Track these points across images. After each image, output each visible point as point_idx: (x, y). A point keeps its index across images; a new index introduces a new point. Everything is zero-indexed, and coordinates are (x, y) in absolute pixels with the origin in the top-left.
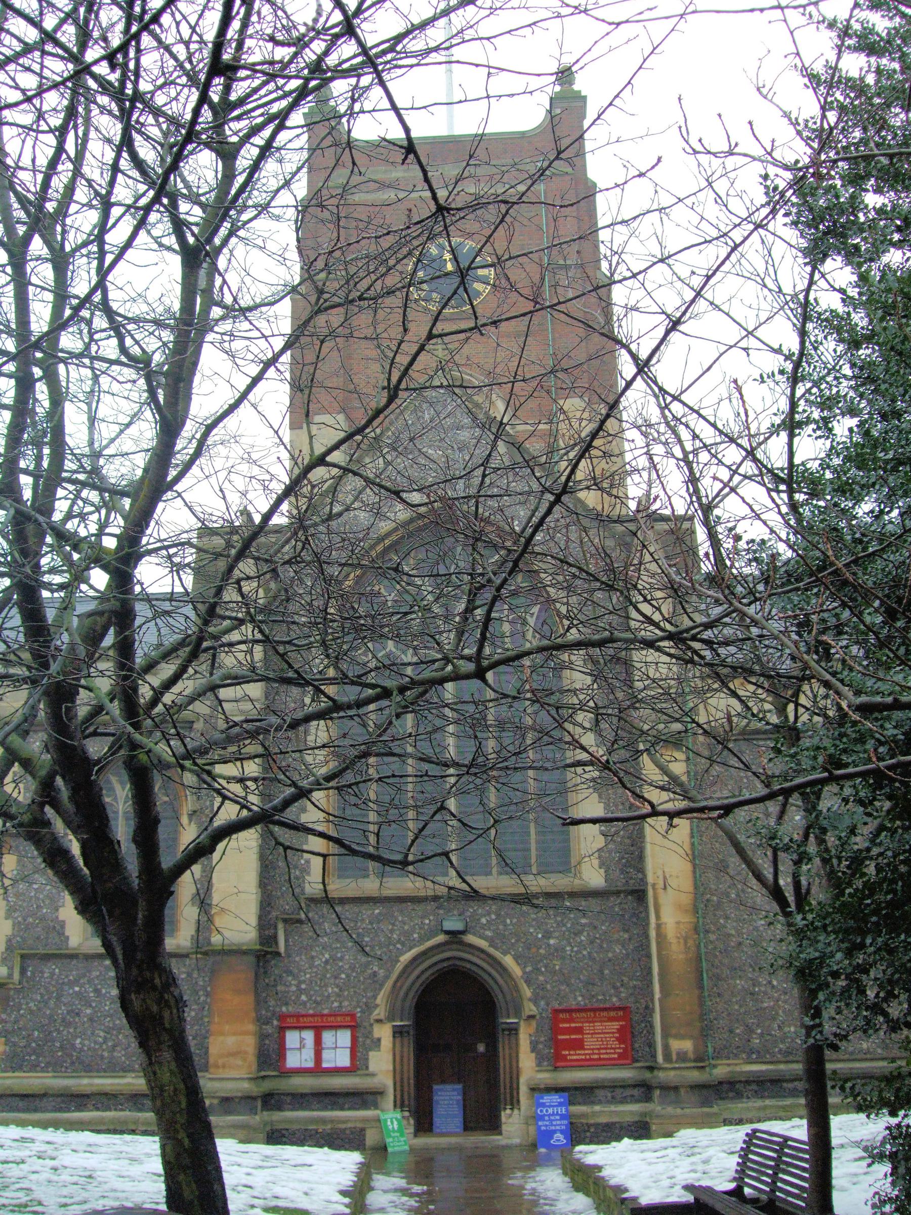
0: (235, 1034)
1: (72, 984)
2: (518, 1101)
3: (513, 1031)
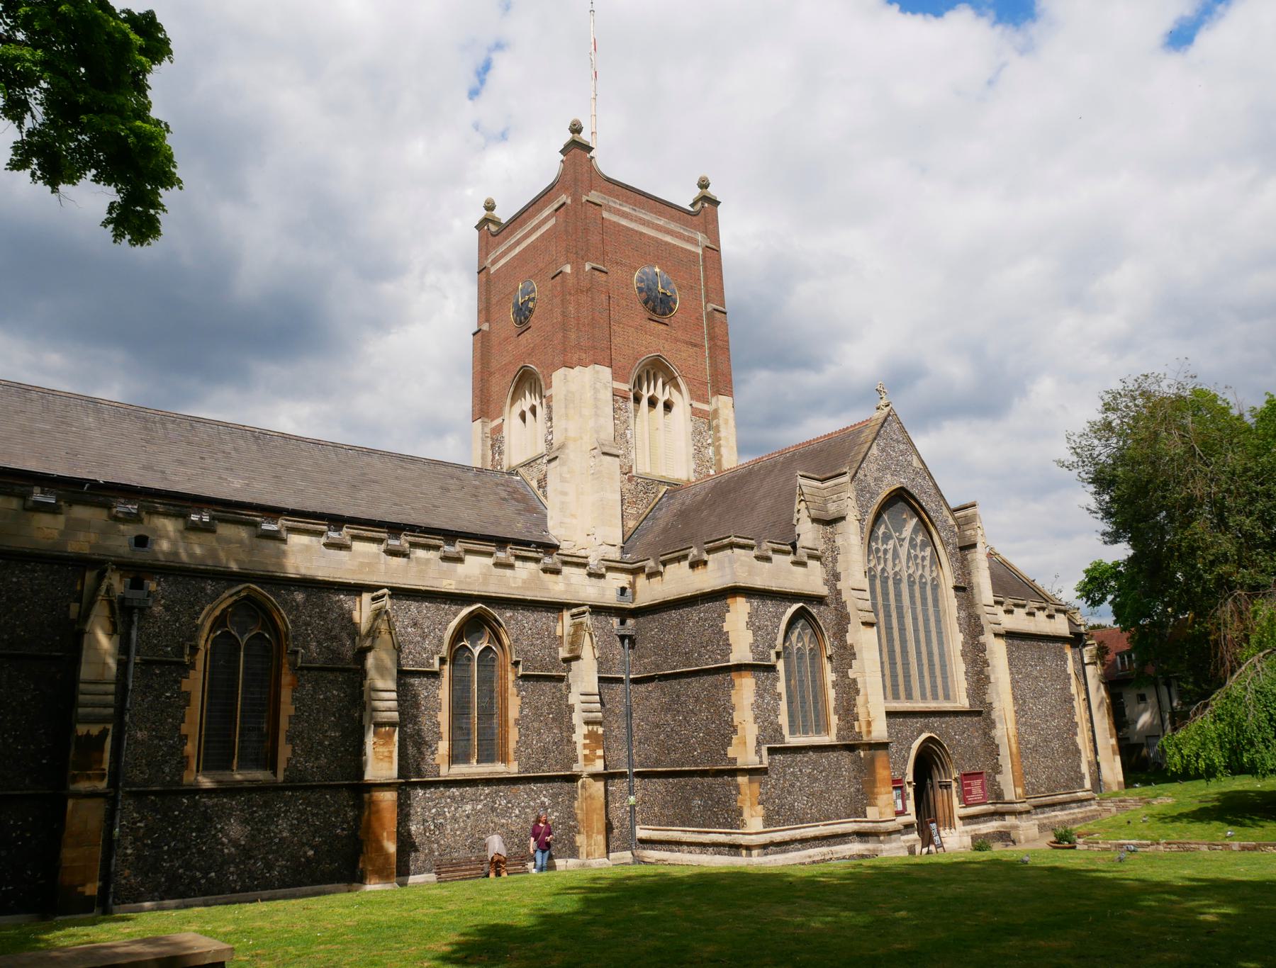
0: (886, 793)
1: (789, 766)
2: (954, 824)
3: (948, 786)
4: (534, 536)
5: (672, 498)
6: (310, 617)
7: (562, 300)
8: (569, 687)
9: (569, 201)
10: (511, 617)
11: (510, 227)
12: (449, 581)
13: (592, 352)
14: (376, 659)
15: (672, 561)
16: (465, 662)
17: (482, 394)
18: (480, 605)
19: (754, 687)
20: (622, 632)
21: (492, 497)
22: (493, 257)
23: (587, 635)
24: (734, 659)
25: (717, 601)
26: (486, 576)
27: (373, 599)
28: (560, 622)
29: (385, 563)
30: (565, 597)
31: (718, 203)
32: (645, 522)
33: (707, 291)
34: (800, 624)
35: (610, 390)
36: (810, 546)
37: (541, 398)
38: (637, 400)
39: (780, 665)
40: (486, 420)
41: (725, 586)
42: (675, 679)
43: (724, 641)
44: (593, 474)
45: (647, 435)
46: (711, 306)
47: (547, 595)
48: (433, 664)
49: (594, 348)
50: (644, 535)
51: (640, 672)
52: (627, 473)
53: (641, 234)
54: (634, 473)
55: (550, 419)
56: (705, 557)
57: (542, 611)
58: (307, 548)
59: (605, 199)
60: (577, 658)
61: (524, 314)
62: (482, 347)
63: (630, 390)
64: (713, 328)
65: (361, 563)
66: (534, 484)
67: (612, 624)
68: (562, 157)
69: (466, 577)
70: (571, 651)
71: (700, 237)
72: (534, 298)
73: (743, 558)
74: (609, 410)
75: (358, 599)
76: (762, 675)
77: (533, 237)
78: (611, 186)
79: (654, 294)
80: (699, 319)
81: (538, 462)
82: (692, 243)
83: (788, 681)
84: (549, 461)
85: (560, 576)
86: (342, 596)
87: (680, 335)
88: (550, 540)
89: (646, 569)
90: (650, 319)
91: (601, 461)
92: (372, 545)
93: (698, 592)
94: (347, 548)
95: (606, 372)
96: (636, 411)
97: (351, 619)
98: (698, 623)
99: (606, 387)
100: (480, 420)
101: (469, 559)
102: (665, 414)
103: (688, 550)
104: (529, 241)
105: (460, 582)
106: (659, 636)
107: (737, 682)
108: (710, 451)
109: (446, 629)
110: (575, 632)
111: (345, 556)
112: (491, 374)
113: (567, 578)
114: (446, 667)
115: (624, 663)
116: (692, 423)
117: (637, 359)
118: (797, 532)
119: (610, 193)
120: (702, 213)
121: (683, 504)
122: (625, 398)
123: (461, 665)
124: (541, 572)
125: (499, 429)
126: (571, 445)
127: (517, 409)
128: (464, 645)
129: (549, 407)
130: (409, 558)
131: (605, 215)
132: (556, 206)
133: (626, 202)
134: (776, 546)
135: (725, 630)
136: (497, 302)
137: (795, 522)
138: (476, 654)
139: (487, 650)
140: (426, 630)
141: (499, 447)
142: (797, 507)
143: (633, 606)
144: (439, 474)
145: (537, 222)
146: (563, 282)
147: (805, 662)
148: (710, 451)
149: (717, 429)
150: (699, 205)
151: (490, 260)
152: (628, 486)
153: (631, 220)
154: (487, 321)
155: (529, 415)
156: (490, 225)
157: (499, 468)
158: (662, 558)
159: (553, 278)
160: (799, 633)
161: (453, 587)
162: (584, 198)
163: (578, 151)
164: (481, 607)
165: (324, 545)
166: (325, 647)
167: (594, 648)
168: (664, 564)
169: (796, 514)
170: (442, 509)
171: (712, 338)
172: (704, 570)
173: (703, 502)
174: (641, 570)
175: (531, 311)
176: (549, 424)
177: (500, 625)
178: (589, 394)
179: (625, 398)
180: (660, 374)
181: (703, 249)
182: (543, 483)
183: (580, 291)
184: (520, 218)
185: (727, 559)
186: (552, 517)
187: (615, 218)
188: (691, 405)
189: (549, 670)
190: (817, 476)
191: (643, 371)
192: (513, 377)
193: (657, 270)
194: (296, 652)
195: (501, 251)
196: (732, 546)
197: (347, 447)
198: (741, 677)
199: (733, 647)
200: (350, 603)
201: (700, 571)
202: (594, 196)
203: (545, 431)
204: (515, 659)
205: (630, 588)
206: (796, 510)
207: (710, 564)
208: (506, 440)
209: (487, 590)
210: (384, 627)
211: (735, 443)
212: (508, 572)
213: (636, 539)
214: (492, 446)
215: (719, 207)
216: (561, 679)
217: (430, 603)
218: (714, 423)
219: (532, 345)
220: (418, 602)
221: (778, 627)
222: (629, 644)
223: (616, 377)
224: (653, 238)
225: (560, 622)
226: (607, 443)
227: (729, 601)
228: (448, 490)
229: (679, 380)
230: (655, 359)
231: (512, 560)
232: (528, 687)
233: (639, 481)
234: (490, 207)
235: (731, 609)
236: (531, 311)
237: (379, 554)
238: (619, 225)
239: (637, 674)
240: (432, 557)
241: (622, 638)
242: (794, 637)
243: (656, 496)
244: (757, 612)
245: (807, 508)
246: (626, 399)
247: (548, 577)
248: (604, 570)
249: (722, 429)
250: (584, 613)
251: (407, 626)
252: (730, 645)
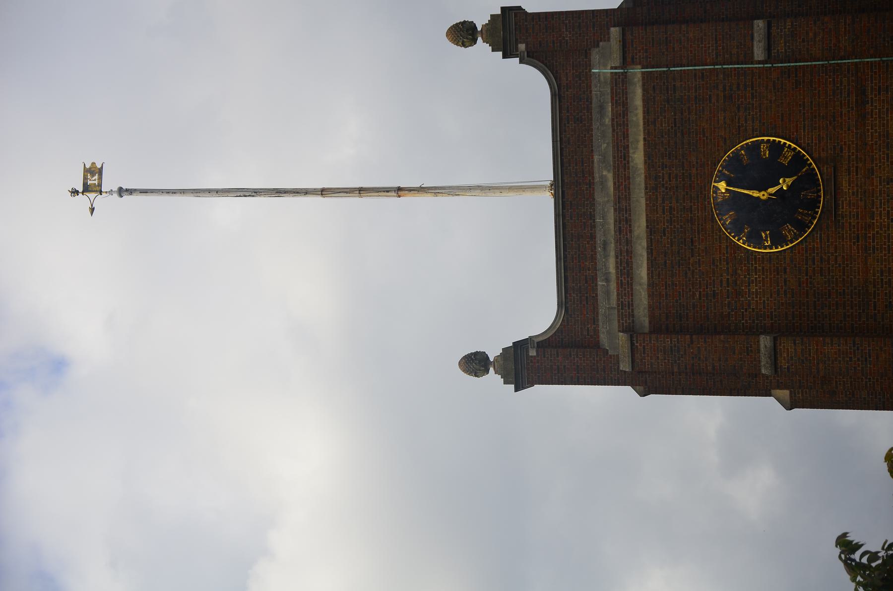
238: (651, 285)
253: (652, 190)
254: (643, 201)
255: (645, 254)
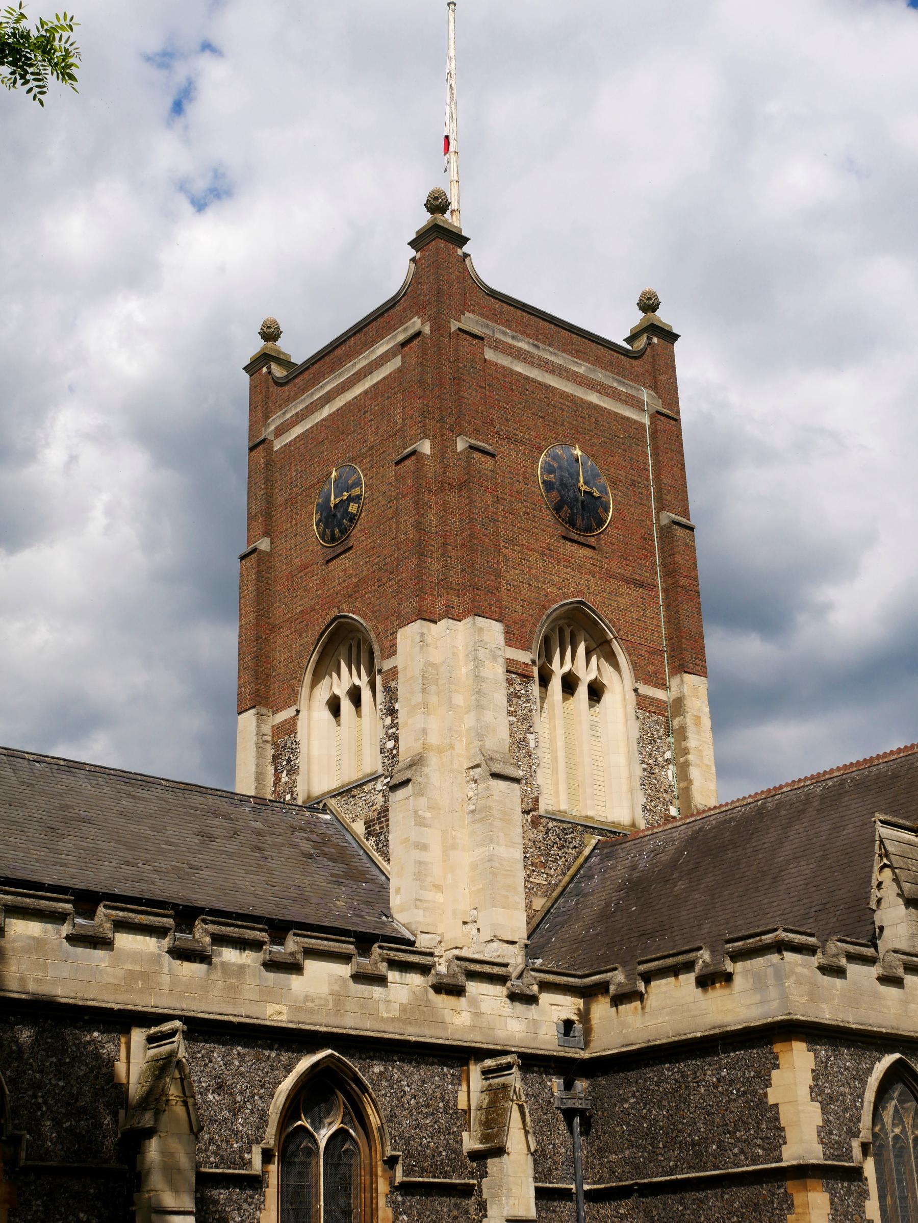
4: (368, 923)
5: (609, 856)
6: (41, 1072)
7: (417, 503)
8: (482, 1207)
9: (427, 330)
10: (381, 1073)
11: (311, 371)
12: (277, 1007)
13: (469, 595)
14: (163, 1152)
15: (662, 973)
16: (303, 1159)
17: (257, 665)
18: (329, 1051)
19: (827, 1209)
20: (570, 1104)
21: (287, 851)
22: (278, 422)
23: (515, 1108)
24: (790, 1155)
25: (753, 1048)
26: (339, 999)
27: (151, 1039)
28: (464, 1087)
29: (170, 972)
30: (471, 1037)
31: (675, 337)
32: (561, 900)
33: (659, 490)
34: (896, 1095)
35: (501, 661)
36: (908, 950)
37: (371, 672)
38: (545, 681)
39: (869, 1168)
40: (264, 711)
41: (769, 1020)
42: (674, 1193)
43: (770, 1121)
44: (473, 812)
45: (560, 744)
46: (667, 517)
47: (439, 1033)
48: (250, 1162)
49: (474, 587)
50: (565, 922)
51: (601, 1180)
52: (531, 808)
53: (549, 388)
54: (542, 810)
55: (392, 712)
56: (729, 966)
57: (432, 1064)
58: (39, 943)
59: (487, 326)
60: (500, 1151)
61: (340, 525)
62: (257, 579)
63: (533, 662)
64: (673, 554)
65: (131, 972)
66: (359, 828)
67: (551, 1088)
68: (412, 253)
69: (307, 998)
70: (485, 1138)
71: (645, 395)
72: (359, 497)
73: (799, 970)
74: (499, 696)
75: (123, 1040)
76: (841, 1186)
77: (358, 390)
78: (498, 305)
79: (571, 494)
80: (647, 538)
81: (367, 788)
82: (633, 406)
83: (882, 1198)
84: (394, 788)
85: (463, 999)
86: (96, 1034)
87: (615, 566)
88: (396, 931)
89: (612, 988)
90: (565, 538)
91: (488, 788)
92: (148, 939)
93: (717, 1031)
94: (106, 944)
95: (494, 631)
96: (543, 699)
97: (111, 1076)
98: (716, 1087)
99: (495, 658)
100: (253, 711)
101: (312, 966)
102: (591, 706)
103: (694, 954)
104: (349, 396)
105: (296, 1009)
106: (639, 1110)
107: (798, 1199)
108: (670, 773)
109: (273, 1096)
110: (493, 1104)
111: (101, 960)
112: (274, 629)
113: (474, 1003)
114: (273, 1168)
115: (573, 1161)
116: (637, 724)
117: (545, 608)
118: (877, 924)
119: (495, 317)
120: (648, 353)
121: (633, 868)
122: (524, 676)
123: (295, 1163)
124: (431, 991)
125: (290, 727)
126: (433, 760)
127: (322, 693)
128: (301, 1125)
129: (391, 694)
130: (210, 963)
131: (489, 354)
132: (401, 338)
133: (523, 333)
134: (851, 948)
135: (771, 1100)
136: (287, 501)
137: (873, 905)
138: (322, 1144)
139: (339, 1136)
140: (238, 1098)
141: (289, 761)
142: (876, 877)
143: (585, 1055)
144: (192, 808)
145: (364, 363)
146: (418, 471)
147: (909, 1162)
148: (670, 773)
149: (682, 734)
150: (644, 339)
151: (272, 428)
152: (532, 834)
153: (532, 364)
154: (267, 534)
155: (346, 705)
156: (274, 366)
157: (288, 797)
158: (642, 968)
159: (398, 463)
160: (896, 1110)
161: (284, 1017)
162: (454, 326)
163: (442, 244)
164: (331, 1055)
165: (69, 938)
166: (66, 1130)
167: (527, 1133)
168: (647, 978)
169: (874, 891)
170: (205, 873)
171: (670, 572)
172: (726, 991)
173: (673, 864)
174: (602, 988)
175: (353, 519)
176: (388, 721)
177: (364, 1089)
178: (464, 670)
179: (524, 676)
180: (582, 635)
181: (652, 417)
182: (377, 827)
183: (445, 486)
184: (332, 356)
185: (770, 971)
186: (398, 890)
187: (504, 361)
188: (636, 690)
189: (446, 1175)
190: (908, 823)
191: (552, 630)
192: (316, 634)
193: (578, 452)
194: (19, 1138)
195: (293, 412)
196: (780, 947)
197: (31, 757)
198: (806, 1189)
199: (789, 1134)
200: (110, 1047)
201: (718, 993)
202: (470, 321)
203: (381, 734)
204: (389, 1152)
205: (580, 1022)
206: (874, 883)
207: (738, 980)
208: (303, 747)
209: (343, 1024)
210: (173, 1091)
211: (712, 759)
212: (377, 991)
213: (548, 930)
214: (275, 757)
215: (676, 344)
216: (466, 1191)
217: (244, 1046)
218: (676, 723)
219: (354, 580)
220: (224, 1045)
221: (861, 1096)
222: (581, 1125)
223: (511, 639)
224: (568, 395)
225: (464, 1087)
226: (497, 756)
227: (777, 1048)
228: (212, 838)
229: (616, 646)
230: (575, 609)
231: (383, 967)
232: (411, 1207)
233: (550, 825)
234: (270, 333)
235: (782, 1061)
236: (353, 519)
237: (159, 955)
238: (512, 373)
239: (594, 1183)
240: (249, 961)
241: (569, 1114)
242: (888, 1115)
243: (580, 853)
244: (826, 1068)
245: (896, 880)
246: (526, 678)
247: (442, 1001)
248: (535, 988)
249: (691, 733)
250: (509, 1066)
251: (207, 1090)
252: (782, 1129)
253: (573, 399)
254: (566, 390)
255: (532, 376)
